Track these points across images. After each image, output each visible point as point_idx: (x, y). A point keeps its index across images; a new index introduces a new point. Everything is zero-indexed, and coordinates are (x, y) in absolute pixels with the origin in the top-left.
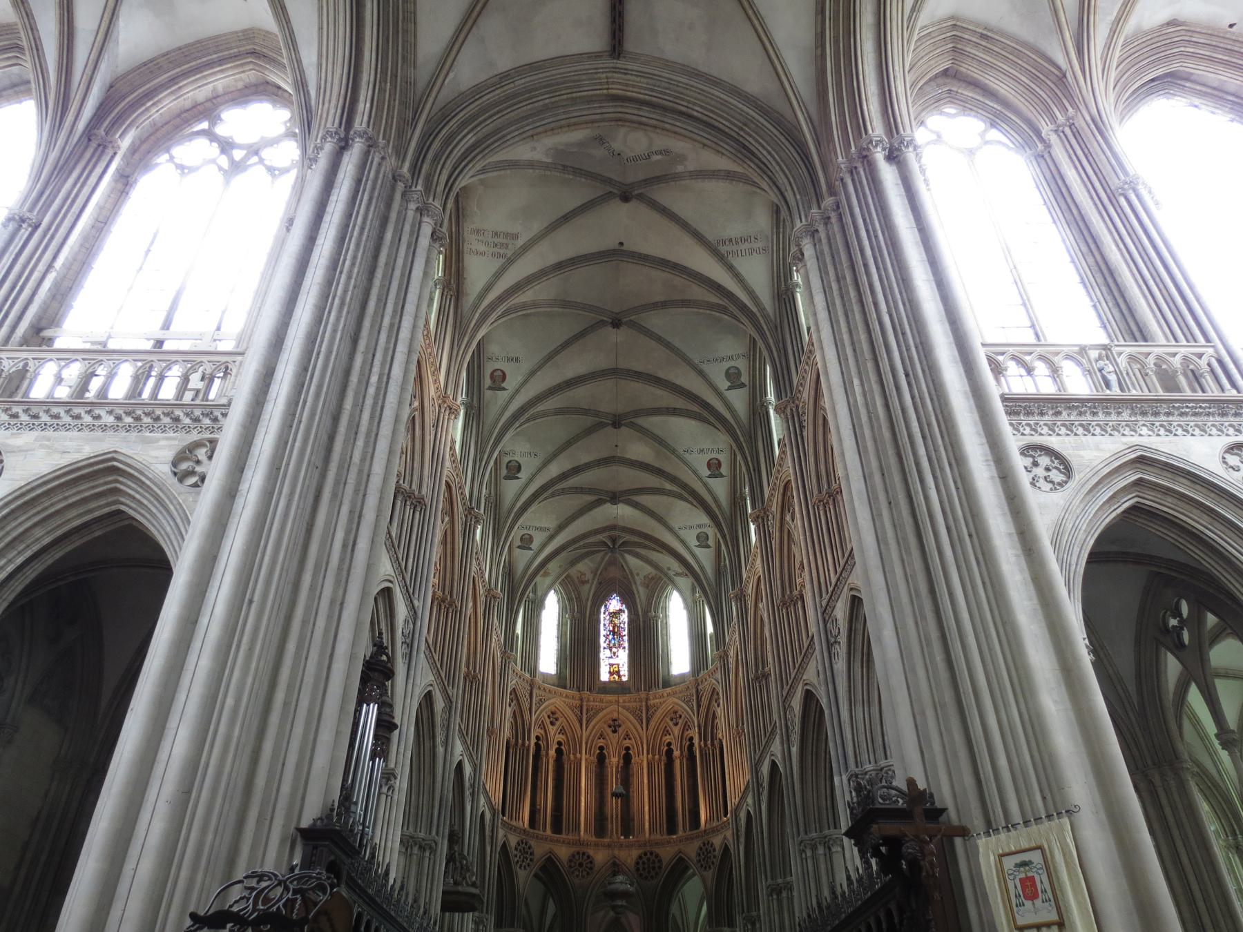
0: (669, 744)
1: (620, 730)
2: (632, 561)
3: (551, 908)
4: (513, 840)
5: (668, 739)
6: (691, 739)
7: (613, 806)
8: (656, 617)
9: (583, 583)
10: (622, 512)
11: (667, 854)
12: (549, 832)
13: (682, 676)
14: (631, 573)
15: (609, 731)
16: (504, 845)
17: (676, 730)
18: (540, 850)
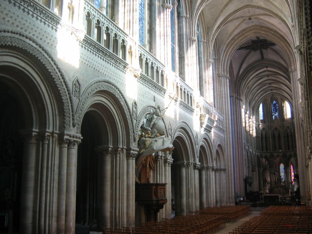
0: (288, 133)
1: (278, 130)
2: (277, 96)
3: (267, 162)
4: (259, 154)
5: (287, 132)
6: (292, 132)
7: (277, 145)
8: (284, 106)
9: (267, 100)
10: (273, 91)
11: (288, 154)
12: (265, 151)
13: (290, 118)
14: (277, 97)
15: (275, 131)
16: (258, 156)
17: (289, 131)
18: (264, 155)
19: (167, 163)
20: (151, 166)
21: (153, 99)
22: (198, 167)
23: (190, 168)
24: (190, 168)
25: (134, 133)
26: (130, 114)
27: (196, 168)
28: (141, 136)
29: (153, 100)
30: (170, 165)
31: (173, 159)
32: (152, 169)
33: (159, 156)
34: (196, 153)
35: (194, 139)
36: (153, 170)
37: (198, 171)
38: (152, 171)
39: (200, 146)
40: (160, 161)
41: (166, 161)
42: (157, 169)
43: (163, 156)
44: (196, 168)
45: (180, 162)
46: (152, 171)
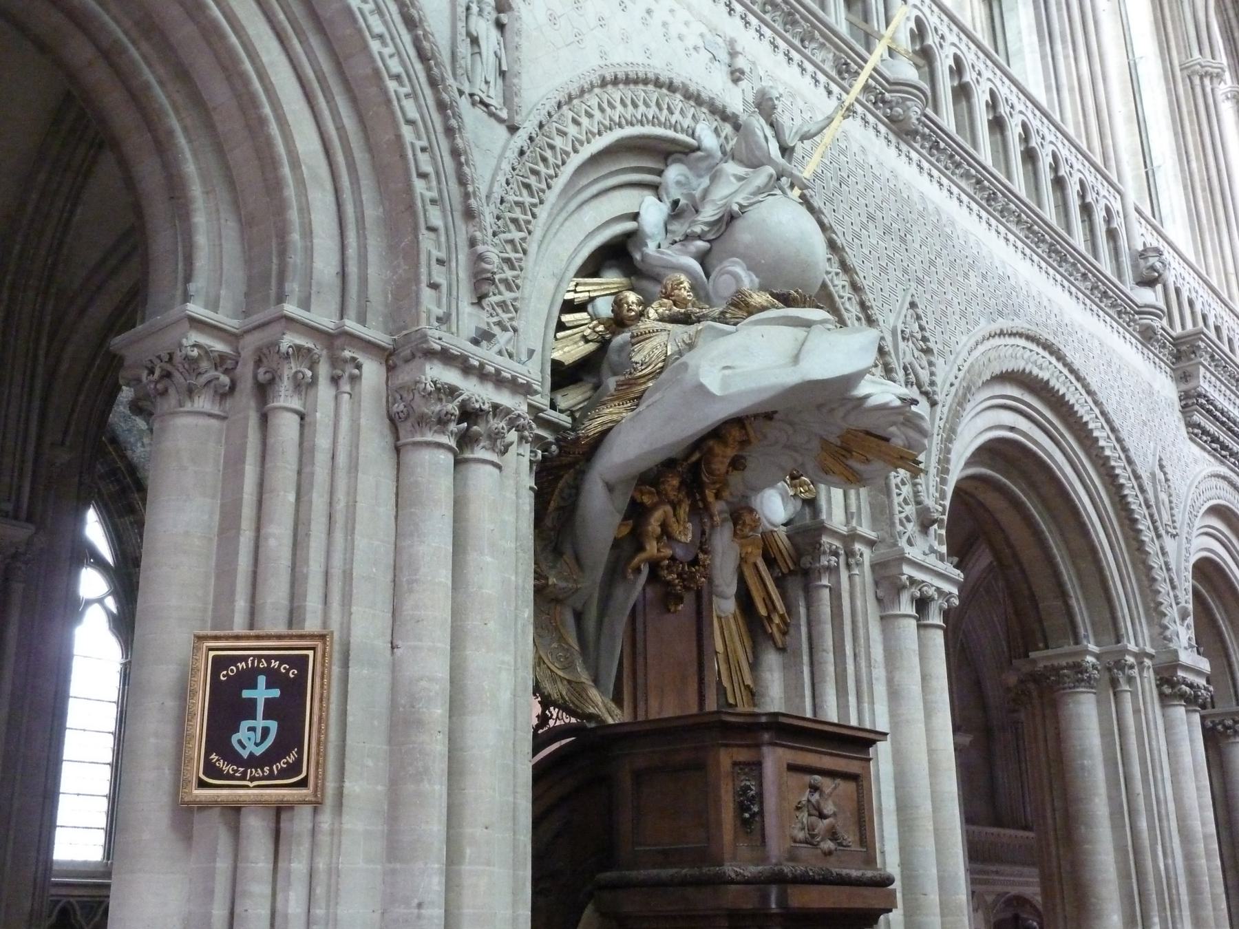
19: (905, 597)
20: (763, 612)
21: (723, 56)
22: (1191, 686)
23: (1134, 695)
24: (1134, 695)
25: (470, 214)
26: (417, 43)
27: (1182, 696)
28: (619, 322)
29: (725, 69)
30: (936, 619)
31: (958, 575)
32: (771, 637)
33: (821, 529)
34: (1164, 588)
35: (1142, 490)
36: (782, 650)
37: (1196, 718)
38: (772, 659)
39: (1193, 559)
40: (833, 571)
41: (888, 581)
42: (821, 635)
43: (865, 530)
44: (1182, 696)
45: (1050, 652)
46: (772, 659)
